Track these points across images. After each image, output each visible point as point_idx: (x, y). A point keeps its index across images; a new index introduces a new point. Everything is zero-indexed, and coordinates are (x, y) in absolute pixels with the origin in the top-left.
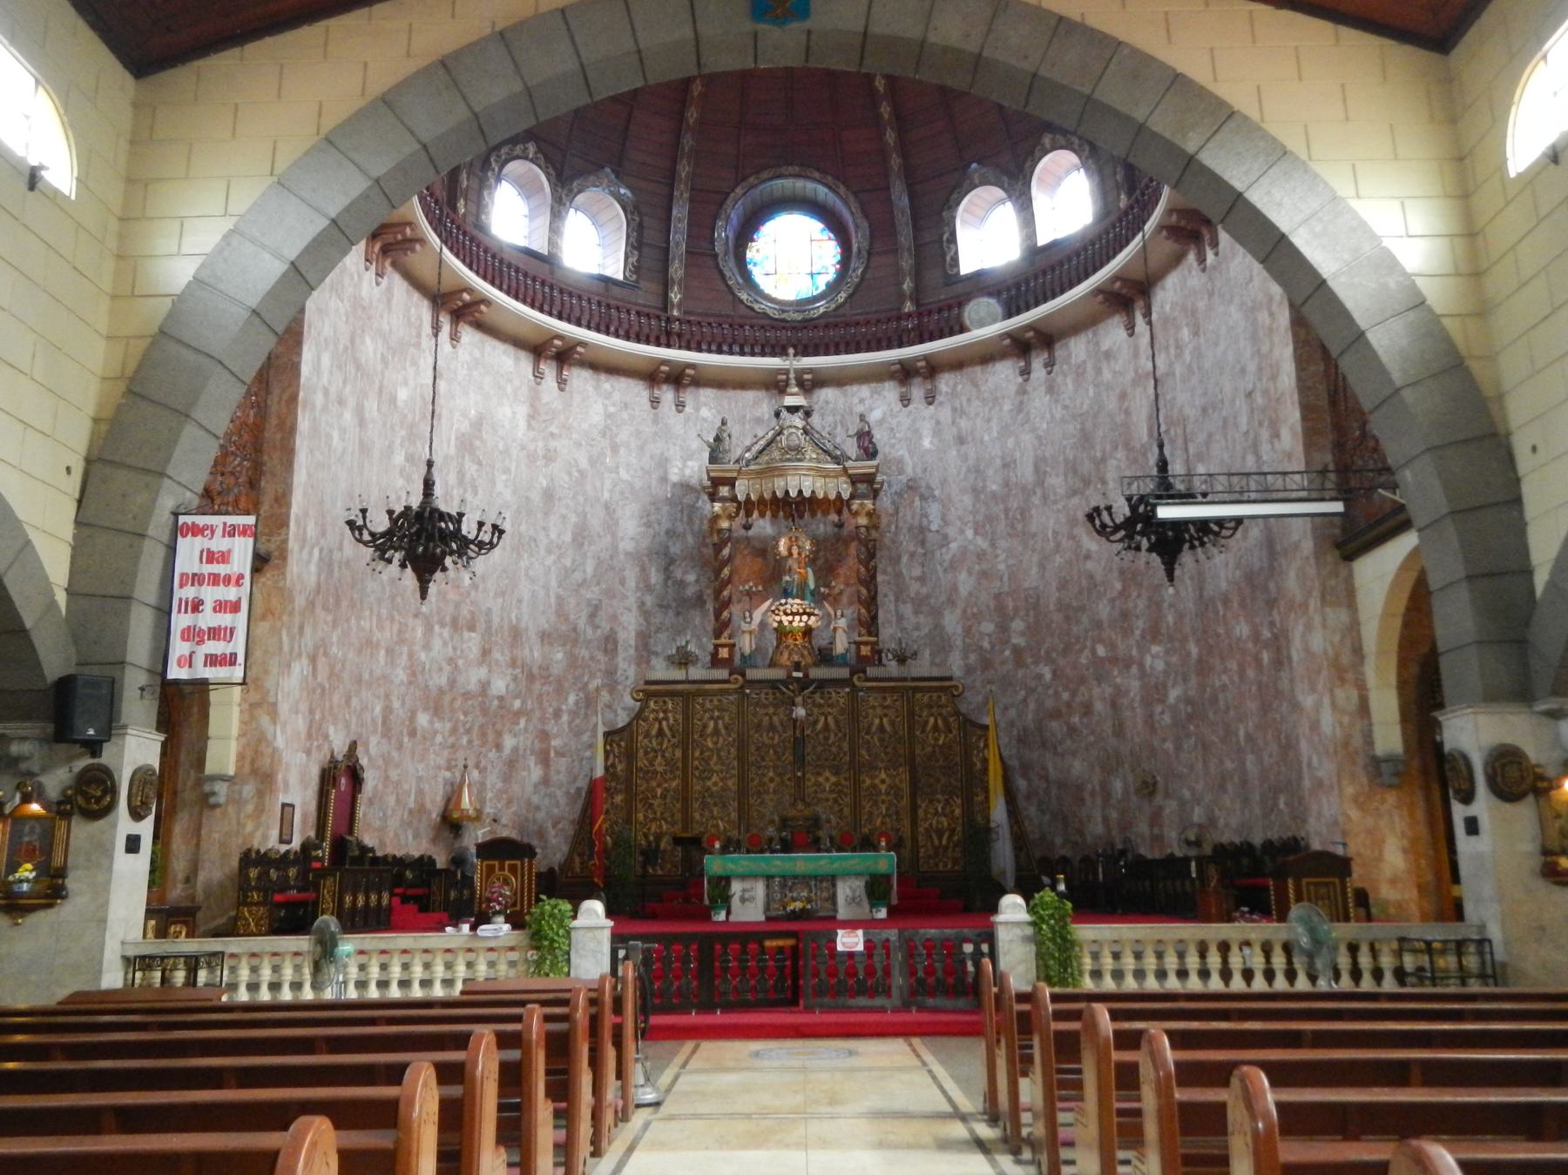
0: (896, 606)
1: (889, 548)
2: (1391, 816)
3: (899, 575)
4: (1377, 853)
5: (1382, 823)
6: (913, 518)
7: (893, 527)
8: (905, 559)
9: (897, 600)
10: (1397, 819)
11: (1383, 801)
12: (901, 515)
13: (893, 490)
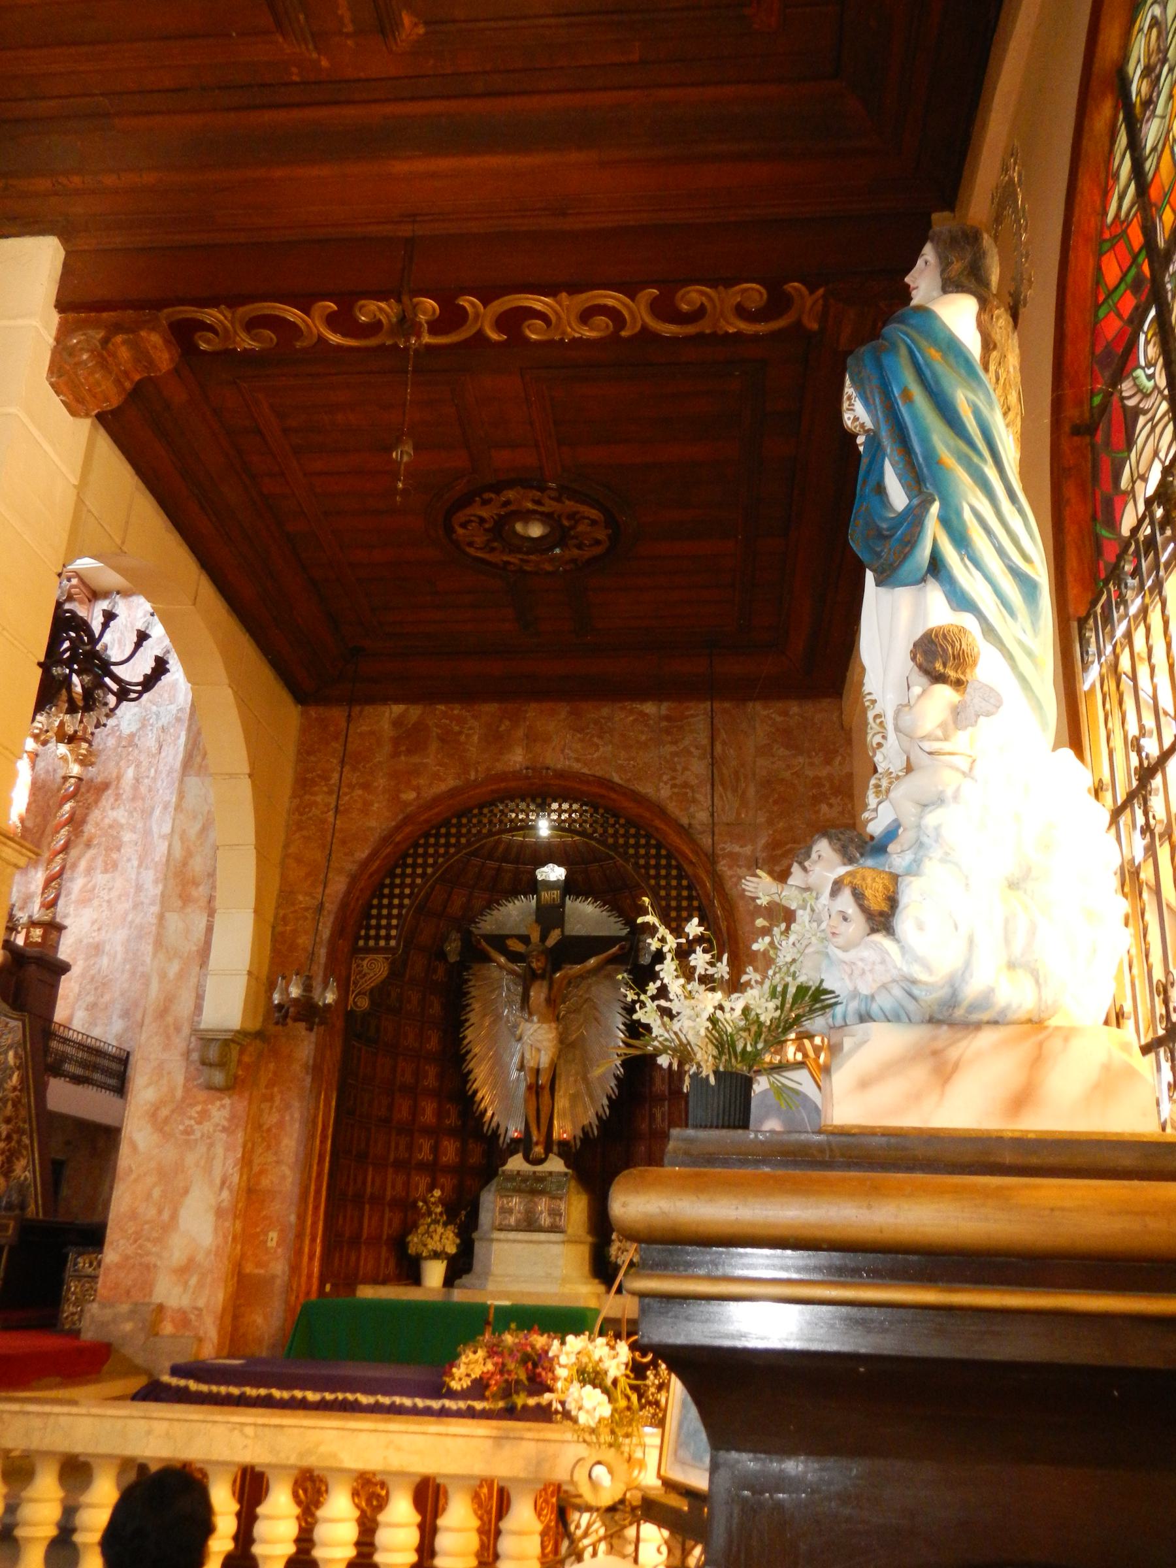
0: (138, 873)
1: (143, 799)
2: (211, 1146)
3: (147, 833)
4: (166, 1215)
5: (191, 1159)
6: (174, 759)
7: (153, 771)
8: (157, 812)
9: (140, 866)
10: (219, 1150)
11: (204, 1116)
12: (163, 754)
13: (160, 724)
